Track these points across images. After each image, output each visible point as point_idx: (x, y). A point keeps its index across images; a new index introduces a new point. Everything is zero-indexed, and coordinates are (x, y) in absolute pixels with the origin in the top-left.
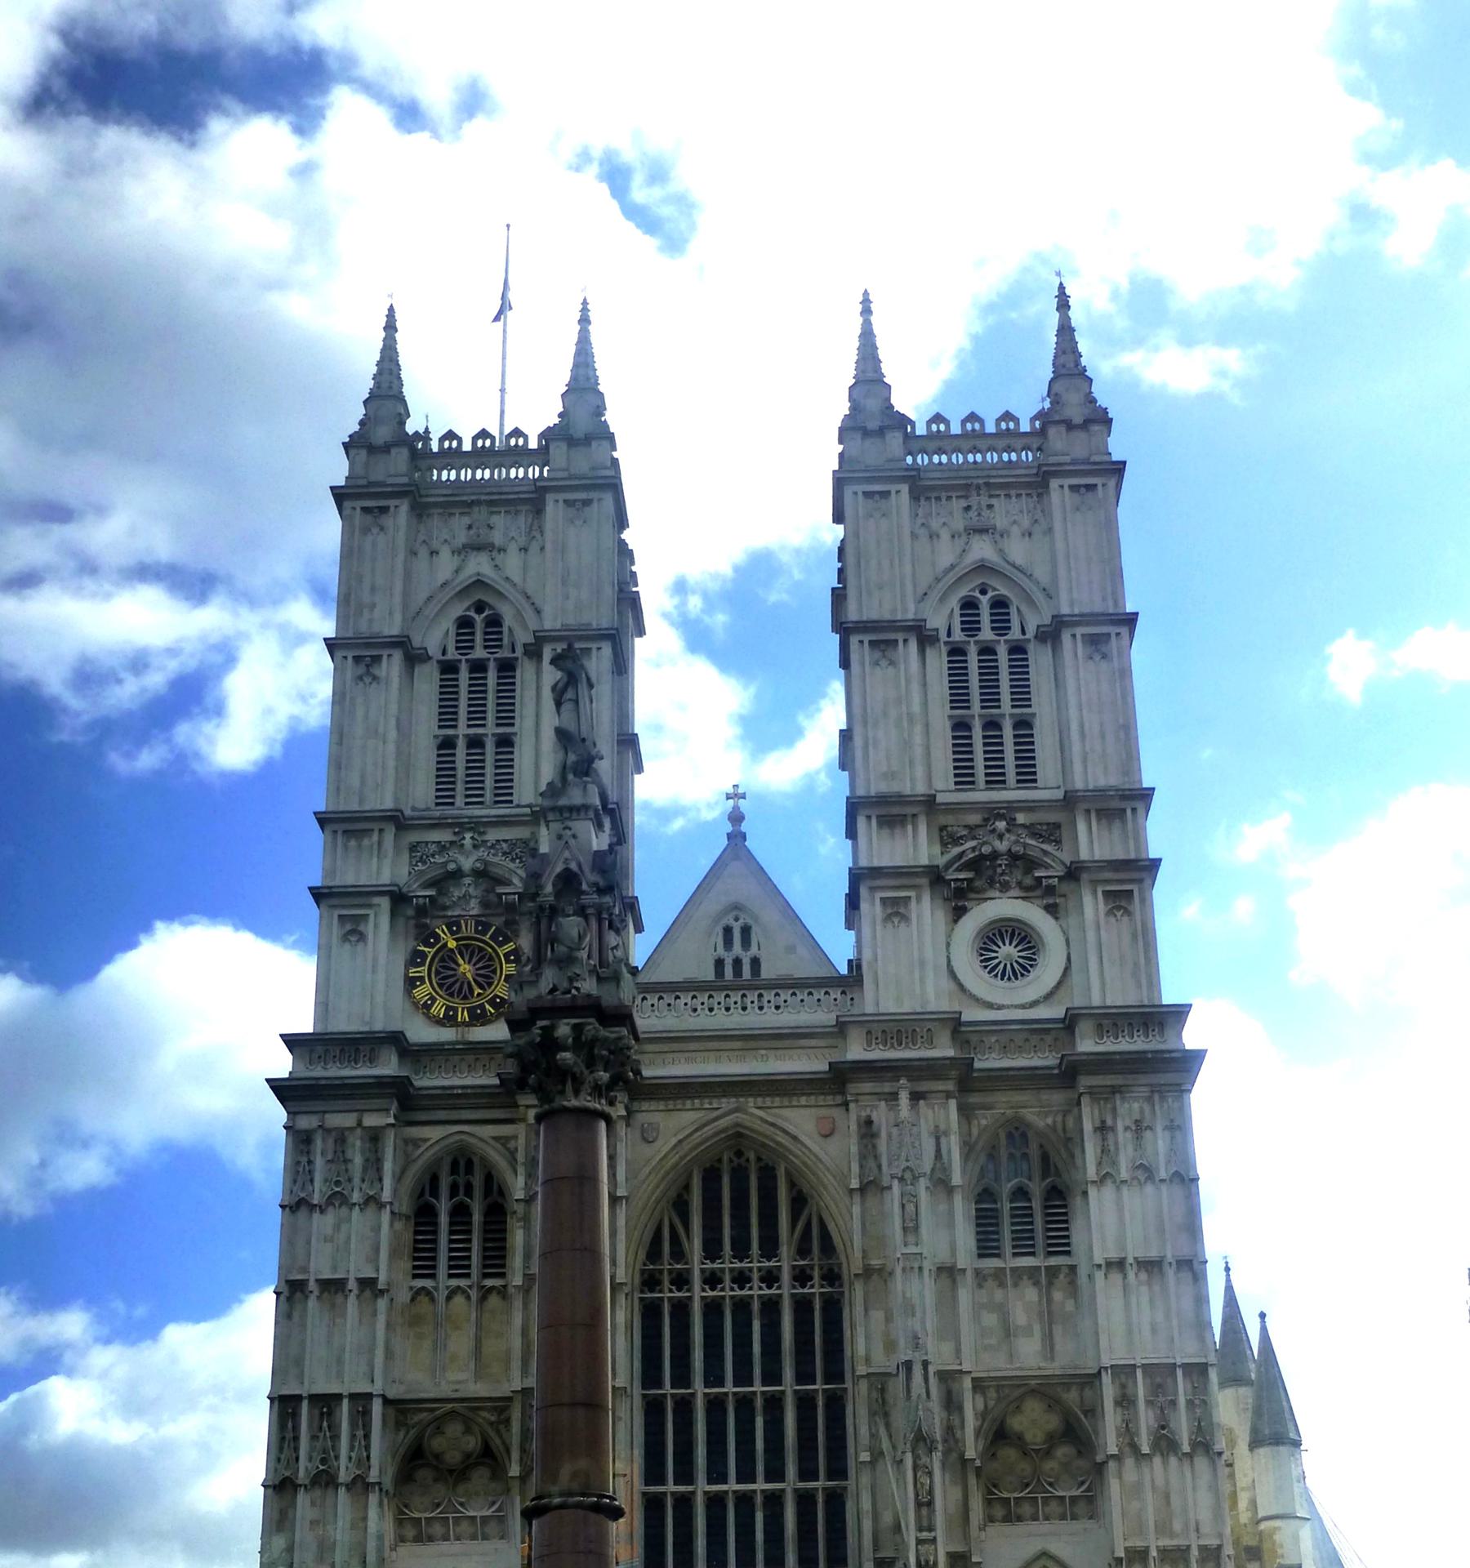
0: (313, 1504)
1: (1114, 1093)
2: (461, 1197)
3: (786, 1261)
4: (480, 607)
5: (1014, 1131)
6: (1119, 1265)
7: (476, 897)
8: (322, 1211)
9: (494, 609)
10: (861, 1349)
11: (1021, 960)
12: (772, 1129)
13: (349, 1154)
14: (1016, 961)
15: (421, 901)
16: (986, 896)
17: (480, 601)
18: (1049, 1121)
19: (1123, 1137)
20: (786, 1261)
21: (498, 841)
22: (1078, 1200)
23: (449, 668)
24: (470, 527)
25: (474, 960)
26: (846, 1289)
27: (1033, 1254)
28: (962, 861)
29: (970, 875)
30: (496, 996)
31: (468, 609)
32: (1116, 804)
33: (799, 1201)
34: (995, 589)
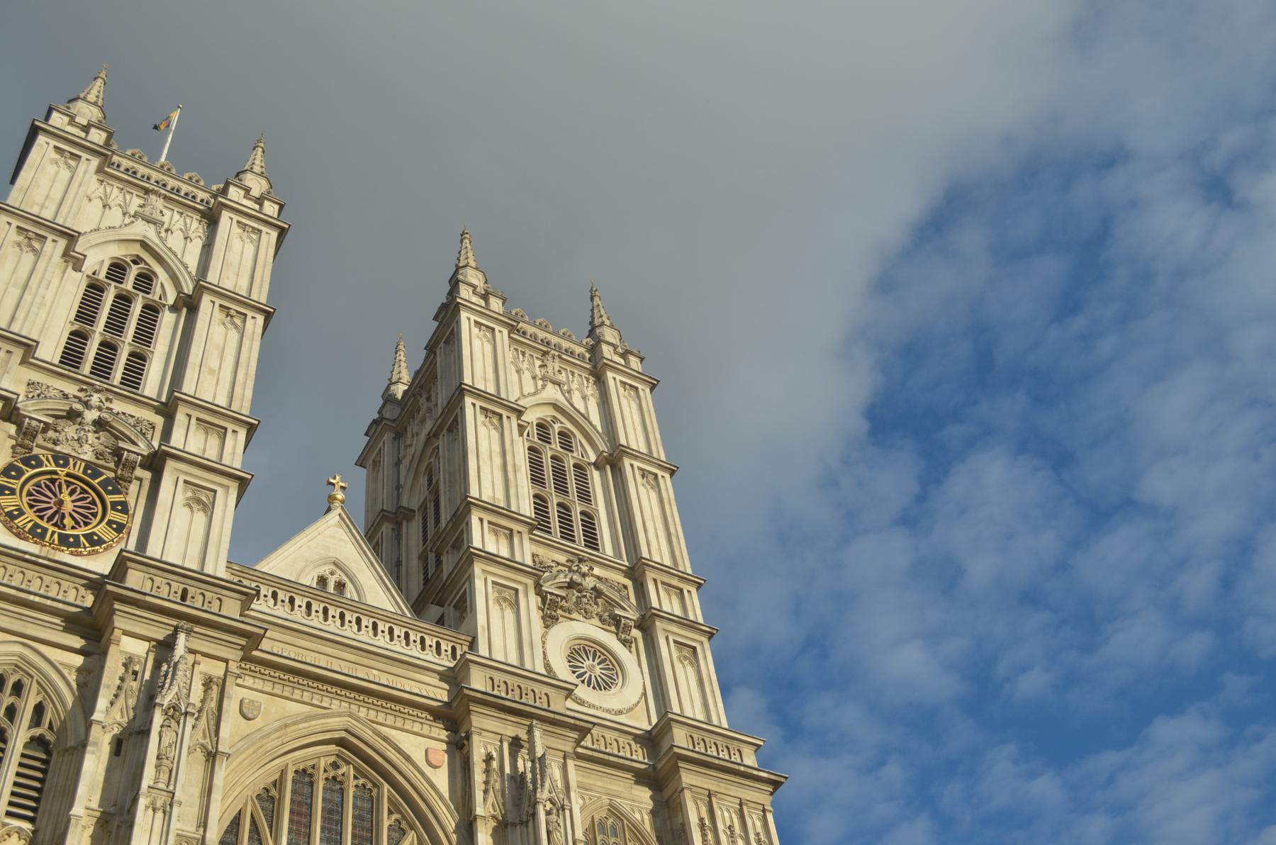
1: (709, 796)
4: (135, 262)
7: (91, 445)
11: (601, 675)
12: (384, 744)
14: (599, 676)
15: (34, 423)
17: (138, 256)
21: (124, 414)
23: (95, 289)
25: (74, 497)
28: (557, 581)
29: (562, 593)
30: (94, 533)
31: (126, 256)
32: (675, 582)
34: (561, 423)
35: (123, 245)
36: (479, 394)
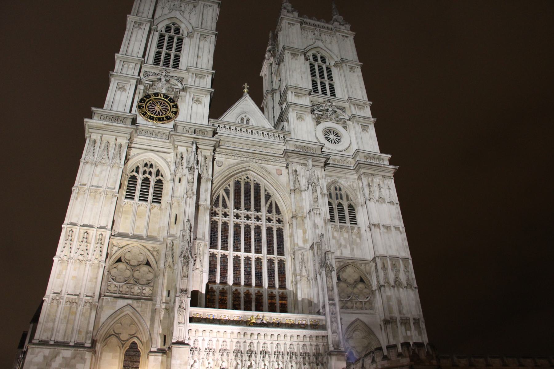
0: (75, 270)
2: (147, 175)
3: (264, 213)
4: (174, 25)
5: (337, 186)
6: (378, 226)
8: (96, 165)
9: (177, 24)
10: (296, 242)
13: (110, 149)
15: (147, 85)
16: (326, 120)
18: (349, 183)
19: (375, 188)
20: (264, 213)
22: (360, 208)
23: (162, 36)
24: (174, 5)
26: (285, 225)
27: (345, 223)
30: (168, 116)
32: (362, 104)
33: (268, 196)
35: (169, 20)
36: (290, 48)
